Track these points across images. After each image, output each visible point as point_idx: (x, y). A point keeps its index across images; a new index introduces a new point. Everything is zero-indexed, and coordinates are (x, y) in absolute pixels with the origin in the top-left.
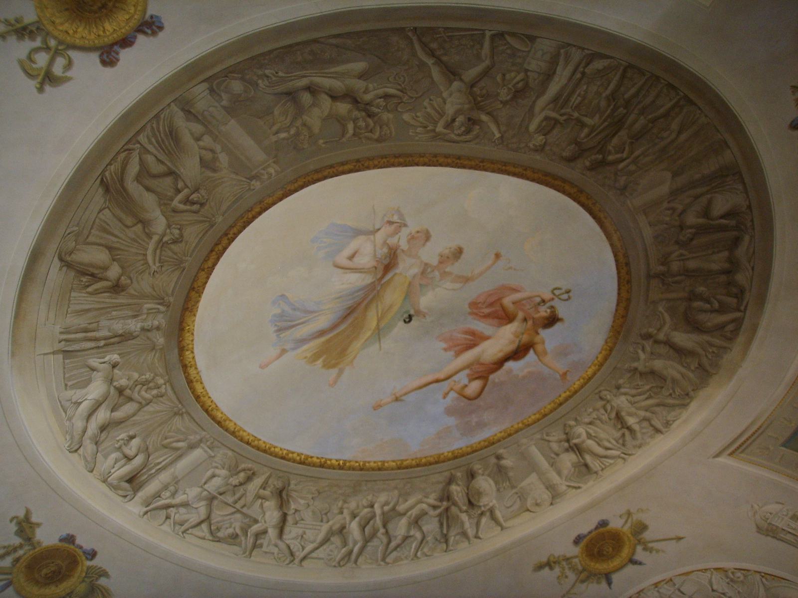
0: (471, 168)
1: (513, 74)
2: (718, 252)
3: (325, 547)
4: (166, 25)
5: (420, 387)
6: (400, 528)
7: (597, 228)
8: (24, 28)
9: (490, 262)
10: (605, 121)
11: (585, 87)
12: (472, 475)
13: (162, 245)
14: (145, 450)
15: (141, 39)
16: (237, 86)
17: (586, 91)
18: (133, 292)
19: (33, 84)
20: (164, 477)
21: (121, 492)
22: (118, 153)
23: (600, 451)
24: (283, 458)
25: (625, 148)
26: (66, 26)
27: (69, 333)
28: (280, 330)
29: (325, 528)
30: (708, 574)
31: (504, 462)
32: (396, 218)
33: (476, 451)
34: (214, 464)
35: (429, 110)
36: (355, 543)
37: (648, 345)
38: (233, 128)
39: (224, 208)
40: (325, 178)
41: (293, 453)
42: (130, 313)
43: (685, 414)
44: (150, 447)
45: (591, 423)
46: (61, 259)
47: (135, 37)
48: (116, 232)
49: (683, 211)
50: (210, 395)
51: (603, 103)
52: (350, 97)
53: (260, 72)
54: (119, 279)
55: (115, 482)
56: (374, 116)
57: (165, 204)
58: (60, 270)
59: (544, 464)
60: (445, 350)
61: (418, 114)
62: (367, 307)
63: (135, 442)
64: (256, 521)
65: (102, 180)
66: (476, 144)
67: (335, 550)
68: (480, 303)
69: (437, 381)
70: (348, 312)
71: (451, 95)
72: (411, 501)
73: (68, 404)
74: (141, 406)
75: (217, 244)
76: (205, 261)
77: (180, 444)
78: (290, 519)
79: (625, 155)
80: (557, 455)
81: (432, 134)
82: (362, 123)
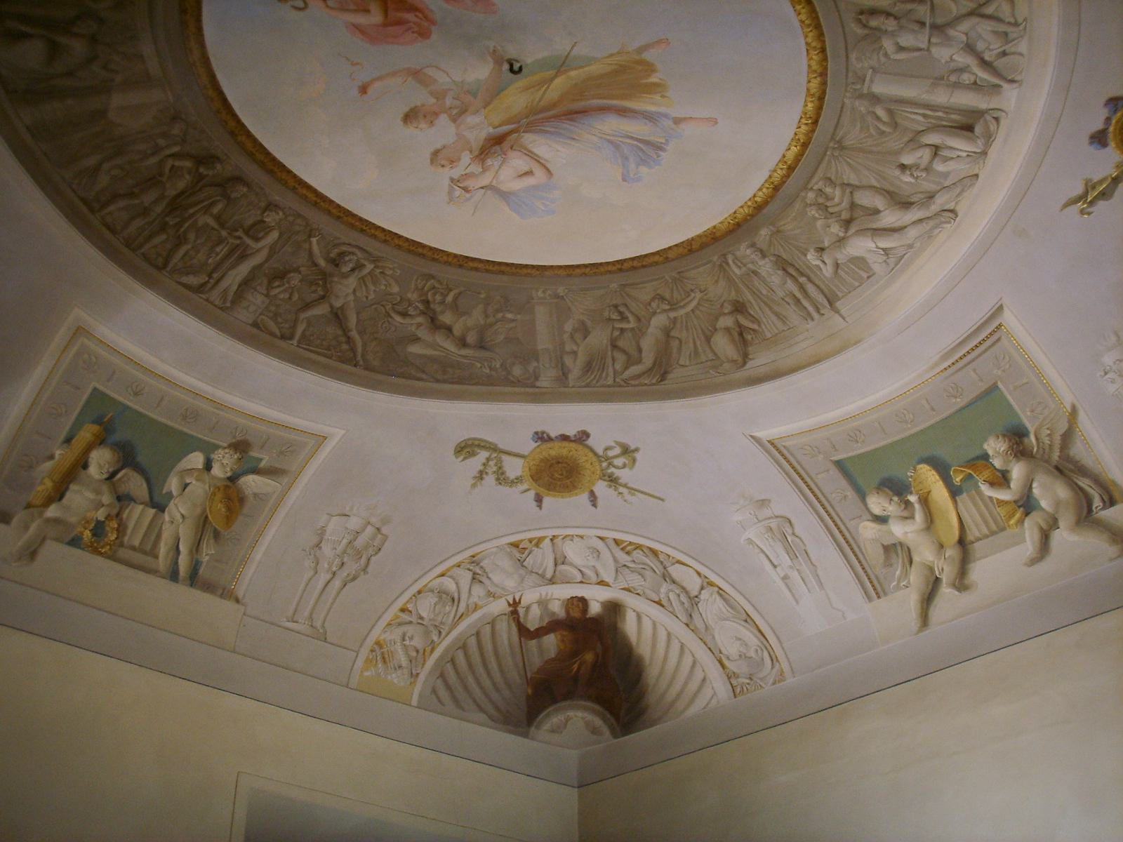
0: (354, 216)
1: (282, 296)
4: (532, 433)
7: (219, 76)
8: (611, 481)
9: (378, 85)
10: (192, 216)
11: (210, 261)
13: (674, 306)
14: (914, 141)
15: (553, 435)
16: (517, 371)
18: (733, 293)
19: (638, 456)
20: (941, 97)
21: (993, 126)
22: (632, 386)
25: (170, 171)
26: (588, 466)
27: (809, 314)
28: (659, 148)
32: (458, 192)
34: (883, 59)
35: (372, 287)
38: (544, 342)
40: (500, 264)
44: (906, 139)
46: (745, 363)
47: (556, 437)
48: (691, 345)
50: (792, 135)
51: (192, 236)
53: (493, 373)
54: (731, 313)
55: (980, 142)
56: (423, 300)
57: (640, 330)
58: (753, 359)
61: (383, 287)
62: (554, 105)
63: (907, 159)
65: (661, 381)
66: (339, 238)
68: (413, 32)
70: (575, 115)
71: (347, 295)
73: (892, 261)
74: (854, 188)
75: (634, 268)
77: (880, 112)
79: (170, 162)
81: (380, 264)
82: (438, 298)
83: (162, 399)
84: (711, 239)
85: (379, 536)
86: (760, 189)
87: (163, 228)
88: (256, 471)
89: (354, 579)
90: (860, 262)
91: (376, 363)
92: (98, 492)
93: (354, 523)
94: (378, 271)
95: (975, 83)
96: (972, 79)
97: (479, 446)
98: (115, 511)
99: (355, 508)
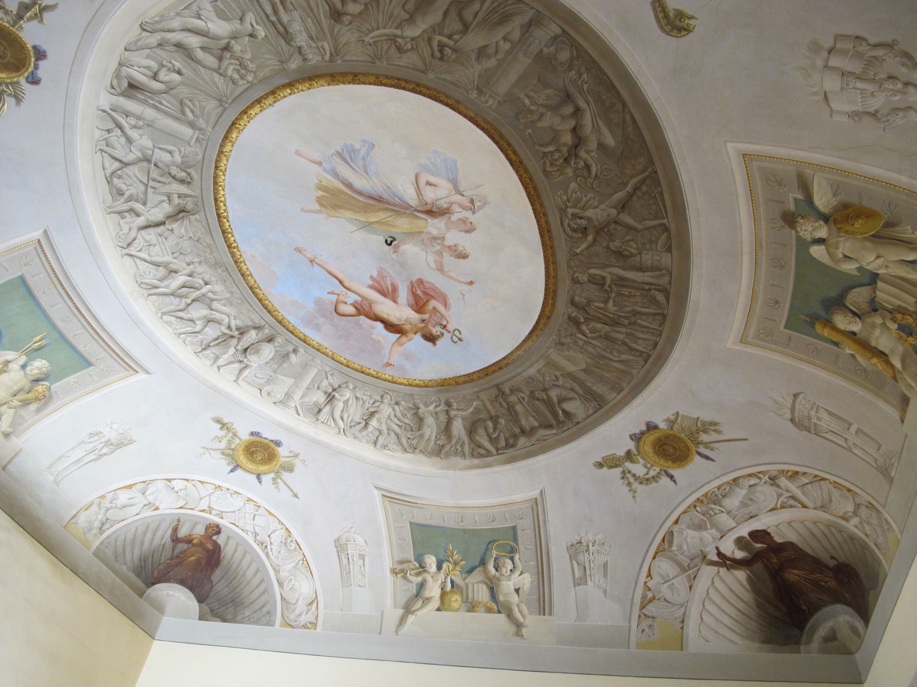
1: (634, 246)
2: (536, 420)
3: (150, 266)
5: (330, 273)
6: (198, 312)
9: (462, 280)
12: (270, 340)
13: (393, 39)
14: (170, 88)
16: (564, 55)
17: (635, 296)
20: (150, 113)
21: (115, 83)
23: (337, 415)
24: (216, 200)
28: (340, 155)
29: (168, 258)
30: (280, 526)
31: (293, 356)
32: (477, 204)
33: (292, 333)
35: (584, 199)
36: (167, 287)
37: (443, 407)
39: (443, 76)
40: (497, 143)
41: (225, 205)
42: (313, 33)
43: (398, 454)
44: (175, 91)
45: (357, 398)
49: (558, 386)
51: (628, 309)
52: (579, 141)
53: (583, 70)
55: (124, 73)
57: (434, 30)
59: (306, 383)
60: (372, 277)
61: (578, 193)
63: (175, 77)
64: (144, 204)
67: (151, 275)
69: (341, 282)
72: (226, 309)
73: (195, 7)
74: (217, 71)
75: (406, 81)
76: (386, 77)
78: (162, 228)
79: (589, 335)
80: (318, 388)
81: (564, 207)
82: (556, 156)
83: (773, 285)
84: (335, 77)
85: (838, 46)
86: (285, 97)
87: (635, 323)
88: (809, 200)
89: (907, 55)
90: (222, 15)
91: (642, 160)
92: (874, 326)
93: (832, 83)
94: (569, 204)
95: (127, 116)
96: (128, 119)
97: (666, 16)
98: (889, 315)
99: (815, 90)
